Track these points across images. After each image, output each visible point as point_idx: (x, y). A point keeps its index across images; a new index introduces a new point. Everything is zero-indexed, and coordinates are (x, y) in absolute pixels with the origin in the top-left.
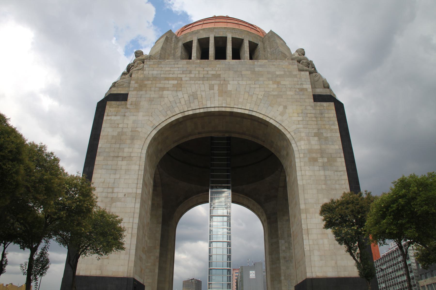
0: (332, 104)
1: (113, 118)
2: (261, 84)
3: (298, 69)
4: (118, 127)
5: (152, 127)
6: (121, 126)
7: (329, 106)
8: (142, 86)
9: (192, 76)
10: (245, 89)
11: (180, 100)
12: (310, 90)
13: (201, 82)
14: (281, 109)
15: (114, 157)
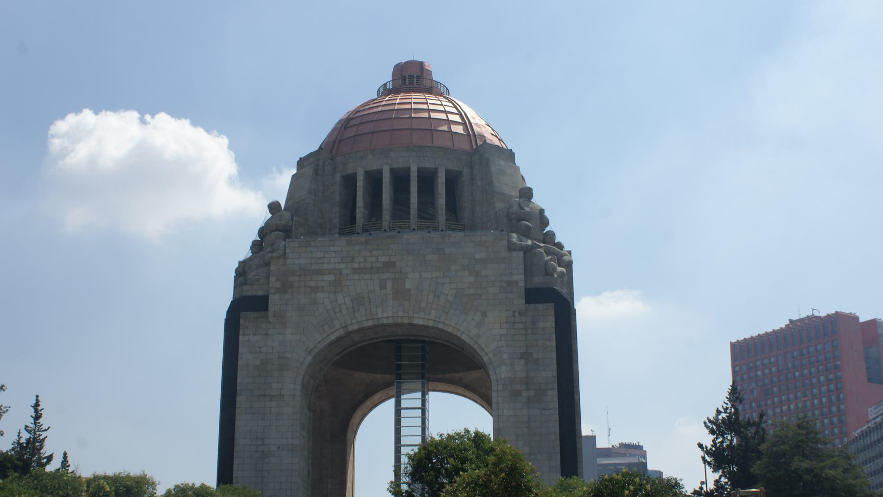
0: (551, 306)
1: (252, 338)
2: (452, 277)
4: (260, 352)
6: (264, 350)
8: (285, 288)
9: (356, 265)
10: (430, 285)
12: (522, 284)
13: (368, 276)
14: (478, 316)
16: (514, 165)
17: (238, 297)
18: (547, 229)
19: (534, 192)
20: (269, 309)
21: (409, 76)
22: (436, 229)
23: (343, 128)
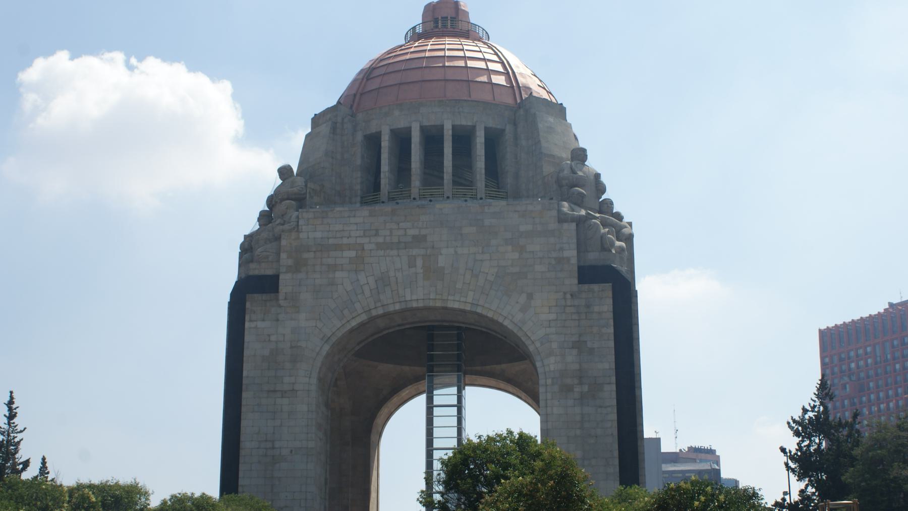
0: (608, 286)
1: (260, 324)
3: (558, 217)
4: (269, 340)
5: (322, 339)
6: (273, 338)
7: (603, 290)
8: (297, 267)
9: (380, 240)
11: (362, 288)
12: (574, 261)
13: (395, 252)
14: (523, 299)
15: (269, 391)
16: (564, 121)
17: (243, 276)
18: (604, 197)
19: (588, 153)
20: (280, 290)
21: (442, 18)
22: (474, 197)
23: (365, 80)
